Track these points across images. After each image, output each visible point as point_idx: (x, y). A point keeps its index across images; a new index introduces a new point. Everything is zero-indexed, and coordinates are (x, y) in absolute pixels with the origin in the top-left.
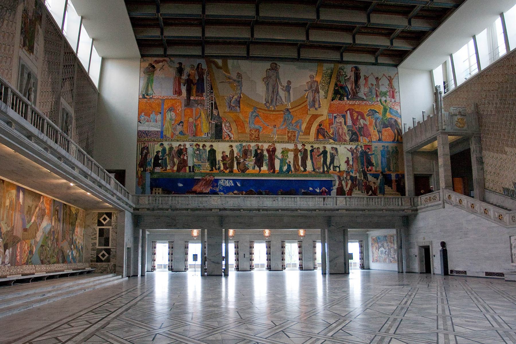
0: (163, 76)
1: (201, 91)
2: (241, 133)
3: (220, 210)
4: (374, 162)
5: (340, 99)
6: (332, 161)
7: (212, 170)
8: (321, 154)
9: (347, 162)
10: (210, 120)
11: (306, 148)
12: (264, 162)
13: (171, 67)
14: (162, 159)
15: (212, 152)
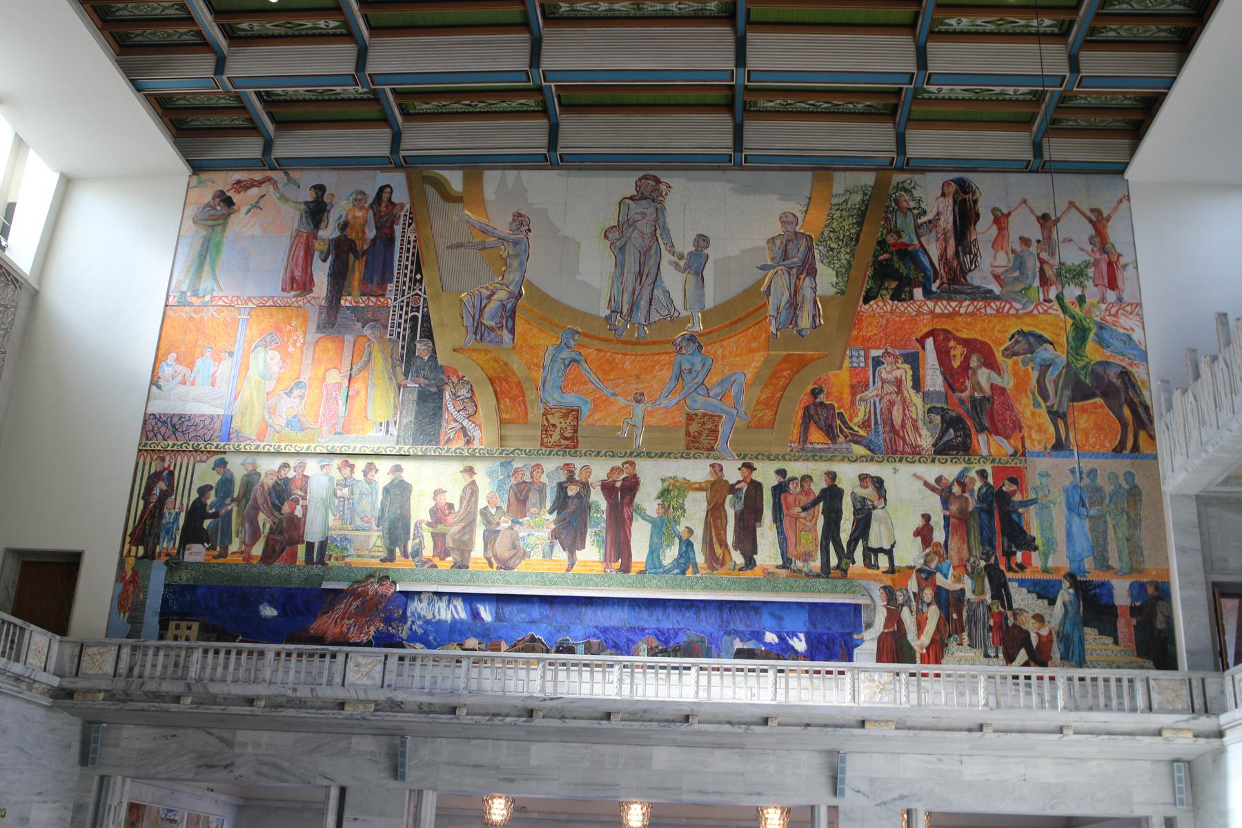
0: (258, 232)
1: (379, 274)
3: (378, 706)
4: (1034, 531)
5: (896, 296)
7: (390, 557)
8: (815, 503)
9: (924, 533)
10: (401, 377)
11: (756, 476)
12: (590, 531)
13: (287, 200)
14: (215, 515)
15: (399, 491)
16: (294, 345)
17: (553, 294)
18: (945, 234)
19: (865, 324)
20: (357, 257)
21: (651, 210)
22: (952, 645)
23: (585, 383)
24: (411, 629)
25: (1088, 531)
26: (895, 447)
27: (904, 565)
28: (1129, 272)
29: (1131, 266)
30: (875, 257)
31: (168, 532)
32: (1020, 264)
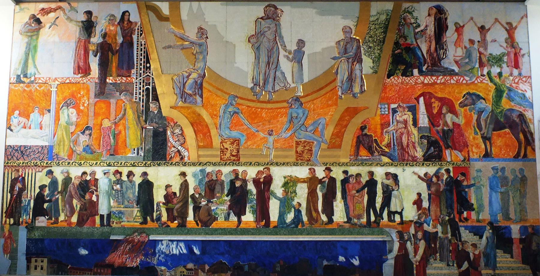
0: (57, 39)
1: (126, 65)
2: (204, 147)
4: (473, 201)
5: (404, 74)
6: (387, 201)
7: (145, 222)
8: (363, 188)
9: (418, 203)
10: (143, 123)
11: (333, 175)
12: (248, 206)
13: (71, 20)
15: (147, 186)
16: (83, 105)
17: (223, 75)
18: (430, 38)
19: (388, 90)
20: (113, 54)
21: (273, 25)
22: (432, 260)
23: (242, 125)
24: (159, 259)
25: (500, 201)
26: (403, 157)
27: (408, 220)
28: (525, 59)
29: (526, 56)
30: (393, 51)
31: (25, 211)
32: (469, 55)
